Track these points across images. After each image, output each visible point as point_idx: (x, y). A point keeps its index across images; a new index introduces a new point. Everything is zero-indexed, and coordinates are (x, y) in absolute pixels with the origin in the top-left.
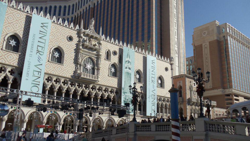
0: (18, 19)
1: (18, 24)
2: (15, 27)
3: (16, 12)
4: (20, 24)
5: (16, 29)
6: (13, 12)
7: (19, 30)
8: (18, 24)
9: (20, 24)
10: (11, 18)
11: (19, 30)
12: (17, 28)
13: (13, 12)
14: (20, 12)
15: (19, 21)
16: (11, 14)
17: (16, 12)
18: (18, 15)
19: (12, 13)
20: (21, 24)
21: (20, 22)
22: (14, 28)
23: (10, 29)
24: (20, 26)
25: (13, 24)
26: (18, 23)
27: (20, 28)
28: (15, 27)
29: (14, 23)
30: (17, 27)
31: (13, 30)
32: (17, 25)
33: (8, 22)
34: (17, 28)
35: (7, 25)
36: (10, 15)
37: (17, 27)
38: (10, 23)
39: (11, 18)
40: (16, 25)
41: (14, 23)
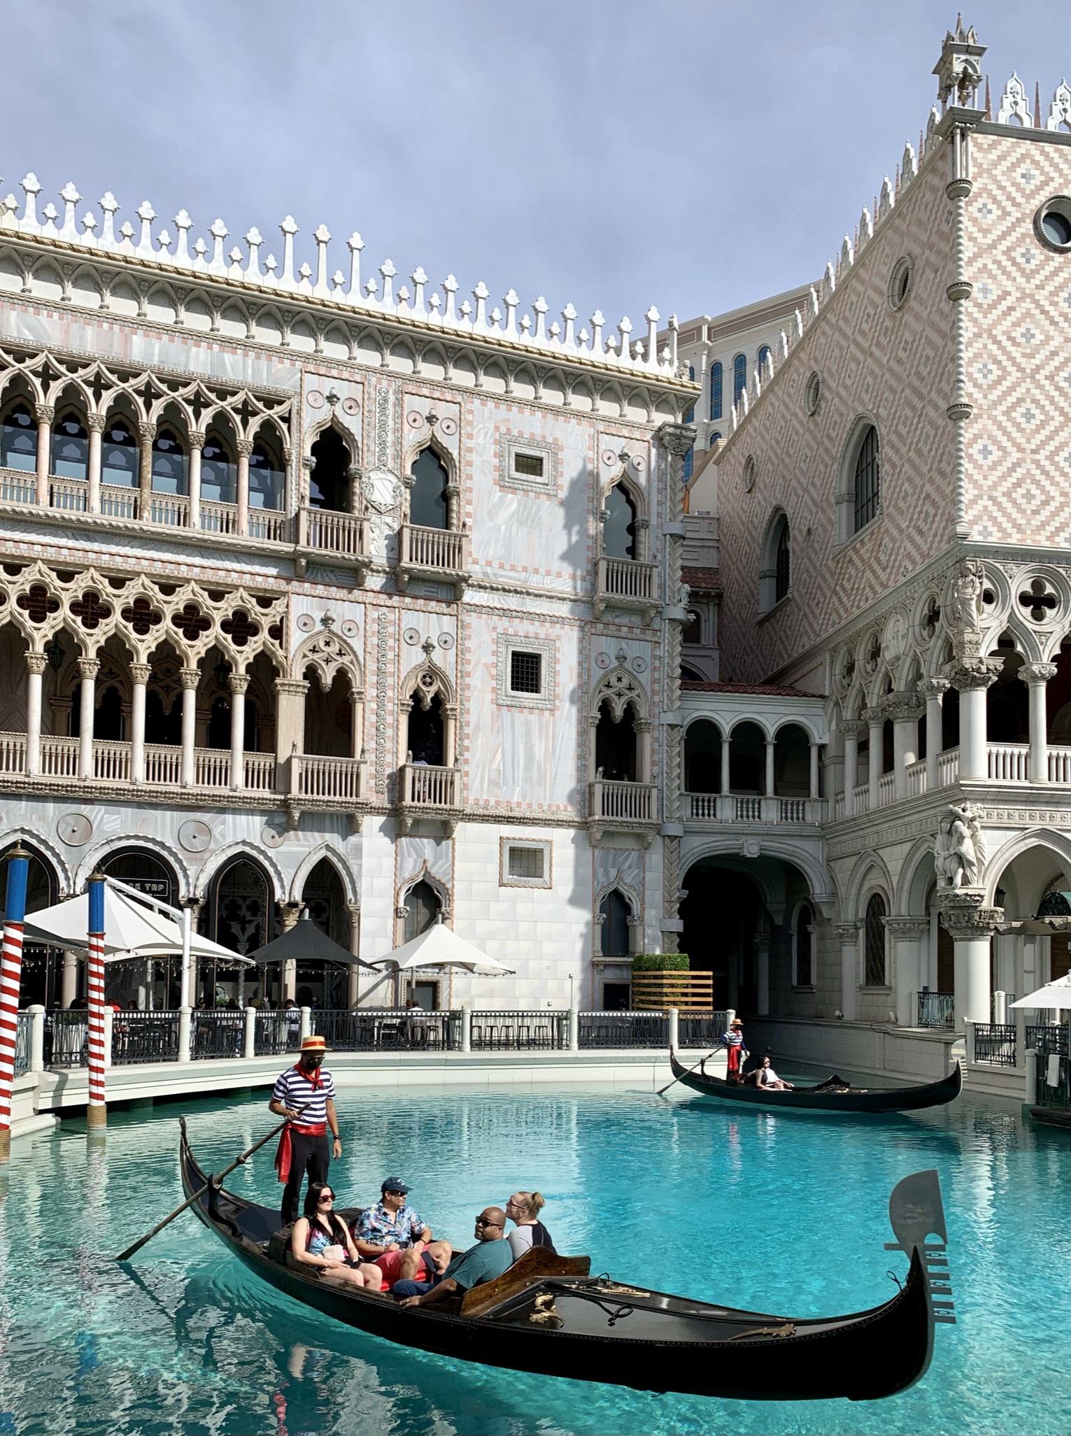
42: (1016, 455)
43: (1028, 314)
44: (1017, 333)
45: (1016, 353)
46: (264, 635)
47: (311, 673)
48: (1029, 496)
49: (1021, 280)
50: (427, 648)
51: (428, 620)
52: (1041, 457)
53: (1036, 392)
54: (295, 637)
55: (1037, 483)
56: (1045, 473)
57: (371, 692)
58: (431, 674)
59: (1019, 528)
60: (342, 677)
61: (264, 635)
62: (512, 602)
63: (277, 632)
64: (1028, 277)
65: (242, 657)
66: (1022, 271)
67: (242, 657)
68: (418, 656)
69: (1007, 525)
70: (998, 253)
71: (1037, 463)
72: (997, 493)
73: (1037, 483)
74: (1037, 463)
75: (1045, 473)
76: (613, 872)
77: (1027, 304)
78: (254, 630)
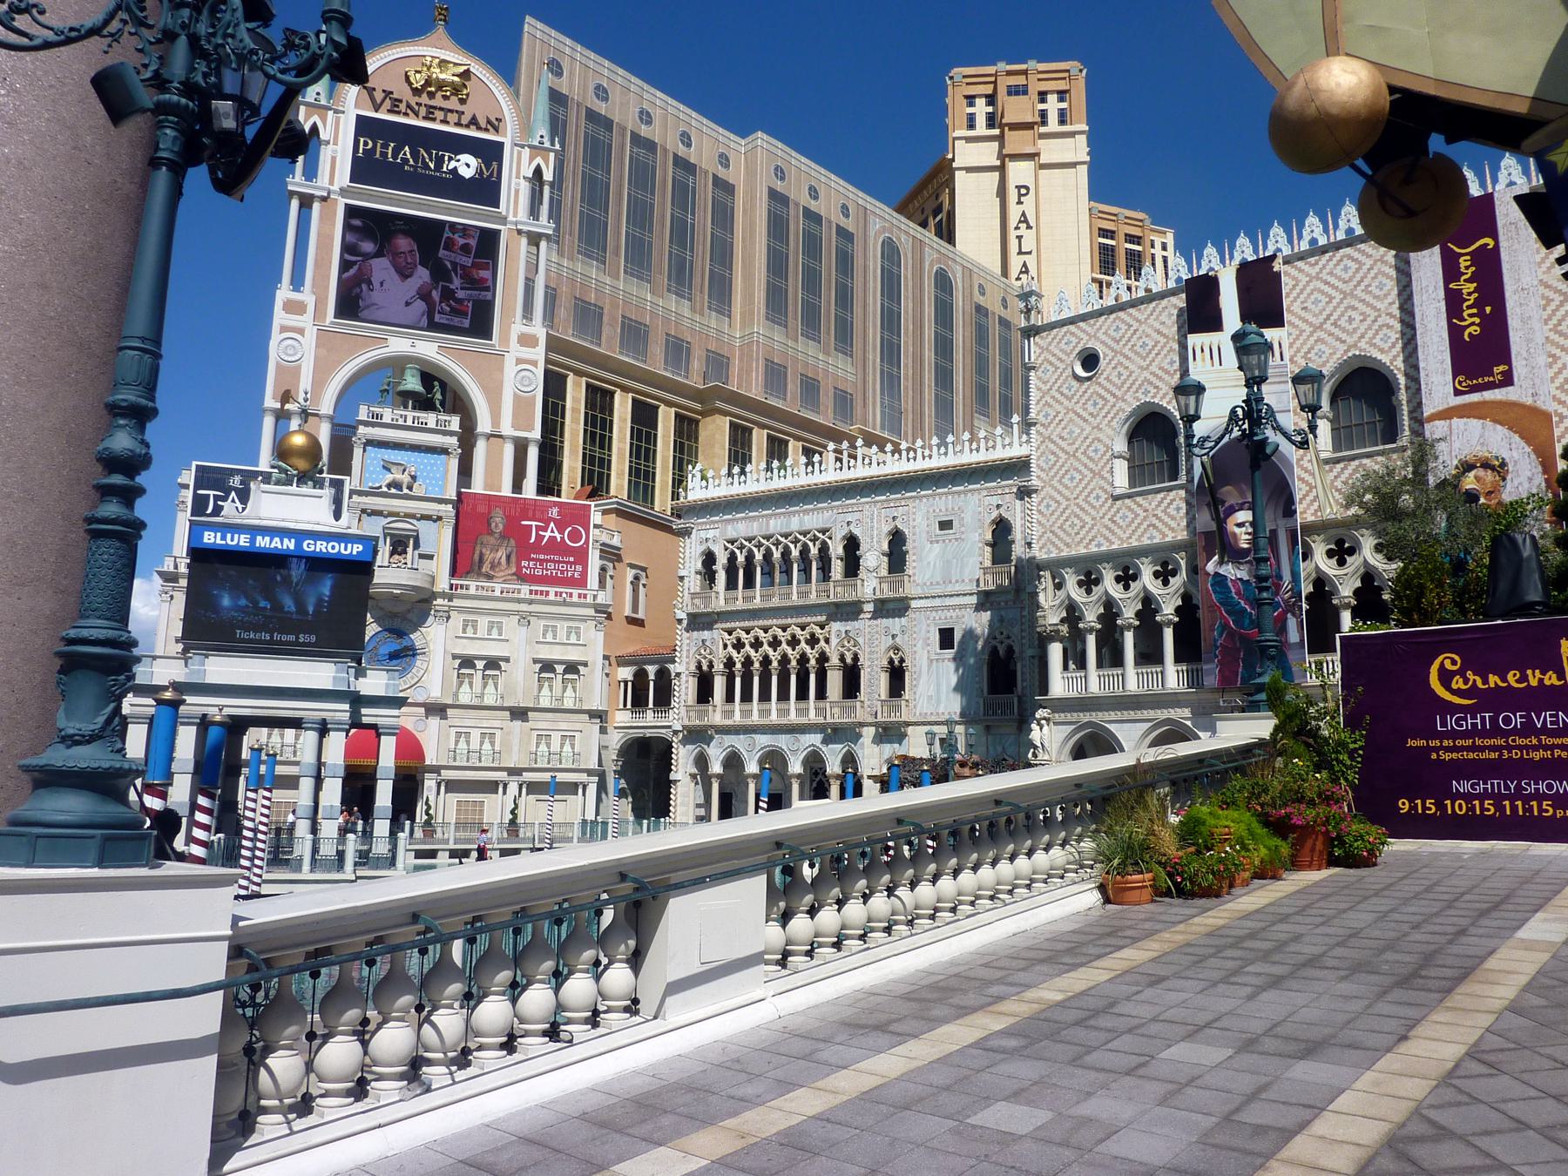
0: (1347, 288)
1: (1354, 308)
2: (1344, 330)
3: (1335, 260)
4: (1368, 305)
5: (1350, 341)
6: (1317, 268)
7: (1370, 334)
8: (1354, 308)
9: (1368, 305)
10: (1316, 302)
11: (1370, 334)
12: (1355, 330)
13: (1317, 268)
14: (1359, 251)
15: (1358, 292)
16: (1312, 286)
17: (1335, 260)
18: (1346, 269)
19: (1318, 278)
20: (1368, 298)
21: (1363, 296)
22: (1344, 336)
23: (1328, 351)
24: (1368, 311)
25: (1335, 324)
26: (1357, 304)
27: (1369, 321)
28: (1344, 330)
29: (1335, 316)
30: (1354, 325)
31: (1343, 347)
32: (1354, 314)
33: (1311, 324)
34: (1355, 330)
35: (1312, 339)
36: (1308, 290)
37: (1354, 325)
38: (1320, 327)
39: (1316, 302)
40: (1351, 320)
41: (1335, 316)
42: (1065, 503)
43: (1071, 420)
44: (1065, 434)
45: (1063, 444)
46: (822, 643)
47: (842, 659)
48: (1073, 525)
49: (1066, 403)
50: (894, 637)
51: (895, 624)
52: (1080, 501)
53: (1076, 464)
54: (834, 641)
55: (1077, 516)
56: (1082, 509)
57: (867, 663)
58: (897, 649)
59: (1068, 545)
60: (856, 658)
61: (822, 643)
62: (937, 602)
63: (827, 641)
64: (1069, 399)
65: (812, 654)
66: (1066, 397)
67: (812, 654)
68: (891, 642)
69: (1061, 545)
70: (1053, 392)
71: (1078, 505)
72: (1055, 528)
73: (1077, 516)
74: (1078, 505)
75: (1082, 509)
76: (1000, 749)
77: (1071, 415)
78: (818, 641)
